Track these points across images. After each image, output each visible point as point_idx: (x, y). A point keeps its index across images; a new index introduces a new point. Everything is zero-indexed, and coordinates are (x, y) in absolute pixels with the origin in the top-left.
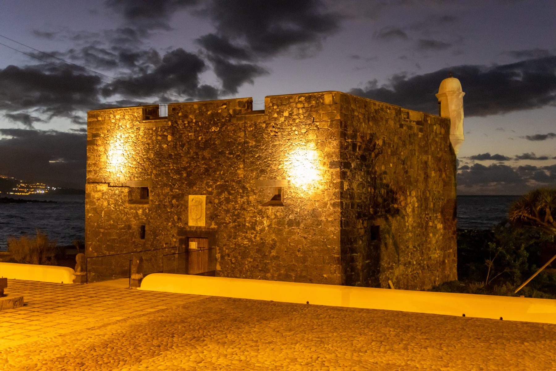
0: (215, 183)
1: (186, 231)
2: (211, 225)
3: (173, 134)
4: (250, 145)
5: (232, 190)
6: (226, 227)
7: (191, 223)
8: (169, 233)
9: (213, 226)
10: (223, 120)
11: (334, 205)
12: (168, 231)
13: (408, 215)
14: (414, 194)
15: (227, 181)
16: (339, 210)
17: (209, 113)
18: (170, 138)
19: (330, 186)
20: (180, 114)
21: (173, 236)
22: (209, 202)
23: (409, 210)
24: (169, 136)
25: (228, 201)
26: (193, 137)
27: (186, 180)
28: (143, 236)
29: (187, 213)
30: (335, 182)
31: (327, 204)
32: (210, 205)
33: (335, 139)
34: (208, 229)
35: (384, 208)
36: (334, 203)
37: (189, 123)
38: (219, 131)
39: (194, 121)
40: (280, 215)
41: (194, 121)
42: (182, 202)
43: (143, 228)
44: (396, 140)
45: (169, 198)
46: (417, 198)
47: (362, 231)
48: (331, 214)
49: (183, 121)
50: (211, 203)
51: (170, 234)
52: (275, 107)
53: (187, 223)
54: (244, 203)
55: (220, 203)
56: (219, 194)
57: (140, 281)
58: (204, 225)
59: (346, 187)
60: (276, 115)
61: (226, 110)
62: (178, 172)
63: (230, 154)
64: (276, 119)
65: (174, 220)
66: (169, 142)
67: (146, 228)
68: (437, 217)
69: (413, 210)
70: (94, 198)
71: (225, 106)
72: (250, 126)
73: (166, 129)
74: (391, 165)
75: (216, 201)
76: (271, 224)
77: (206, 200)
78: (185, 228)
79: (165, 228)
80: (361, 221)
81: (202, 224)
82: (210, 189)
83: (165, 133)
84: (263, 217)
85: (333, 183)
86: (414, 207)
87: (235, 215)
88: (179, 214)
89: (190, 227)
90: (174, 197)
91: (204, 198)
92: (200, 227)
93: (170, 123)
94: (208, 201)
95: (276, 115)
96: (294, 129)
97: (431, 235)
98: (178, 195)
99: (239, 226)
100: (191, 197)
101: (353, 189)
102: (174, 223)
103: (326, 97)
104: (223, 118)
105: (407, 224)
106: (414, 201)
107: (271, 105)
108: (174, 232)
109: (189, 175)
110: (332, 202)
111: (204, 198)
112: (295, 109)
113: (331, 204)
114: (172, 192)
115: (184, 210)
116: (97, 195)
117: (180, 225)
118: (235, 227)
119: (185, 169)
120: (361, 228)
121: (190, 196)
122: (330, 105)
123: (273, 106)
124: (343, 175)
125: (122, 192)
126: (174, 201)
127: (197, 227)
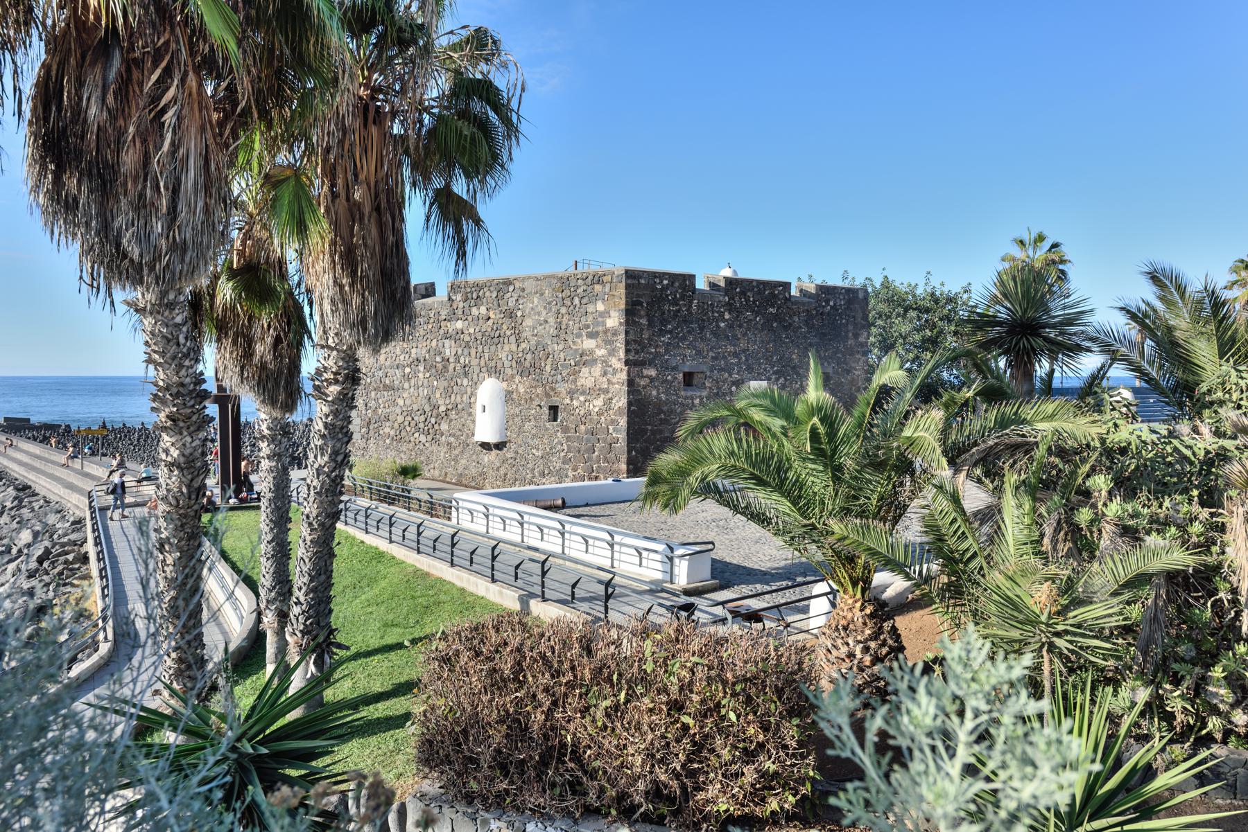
18: (727, 316)
119: (744, 351)
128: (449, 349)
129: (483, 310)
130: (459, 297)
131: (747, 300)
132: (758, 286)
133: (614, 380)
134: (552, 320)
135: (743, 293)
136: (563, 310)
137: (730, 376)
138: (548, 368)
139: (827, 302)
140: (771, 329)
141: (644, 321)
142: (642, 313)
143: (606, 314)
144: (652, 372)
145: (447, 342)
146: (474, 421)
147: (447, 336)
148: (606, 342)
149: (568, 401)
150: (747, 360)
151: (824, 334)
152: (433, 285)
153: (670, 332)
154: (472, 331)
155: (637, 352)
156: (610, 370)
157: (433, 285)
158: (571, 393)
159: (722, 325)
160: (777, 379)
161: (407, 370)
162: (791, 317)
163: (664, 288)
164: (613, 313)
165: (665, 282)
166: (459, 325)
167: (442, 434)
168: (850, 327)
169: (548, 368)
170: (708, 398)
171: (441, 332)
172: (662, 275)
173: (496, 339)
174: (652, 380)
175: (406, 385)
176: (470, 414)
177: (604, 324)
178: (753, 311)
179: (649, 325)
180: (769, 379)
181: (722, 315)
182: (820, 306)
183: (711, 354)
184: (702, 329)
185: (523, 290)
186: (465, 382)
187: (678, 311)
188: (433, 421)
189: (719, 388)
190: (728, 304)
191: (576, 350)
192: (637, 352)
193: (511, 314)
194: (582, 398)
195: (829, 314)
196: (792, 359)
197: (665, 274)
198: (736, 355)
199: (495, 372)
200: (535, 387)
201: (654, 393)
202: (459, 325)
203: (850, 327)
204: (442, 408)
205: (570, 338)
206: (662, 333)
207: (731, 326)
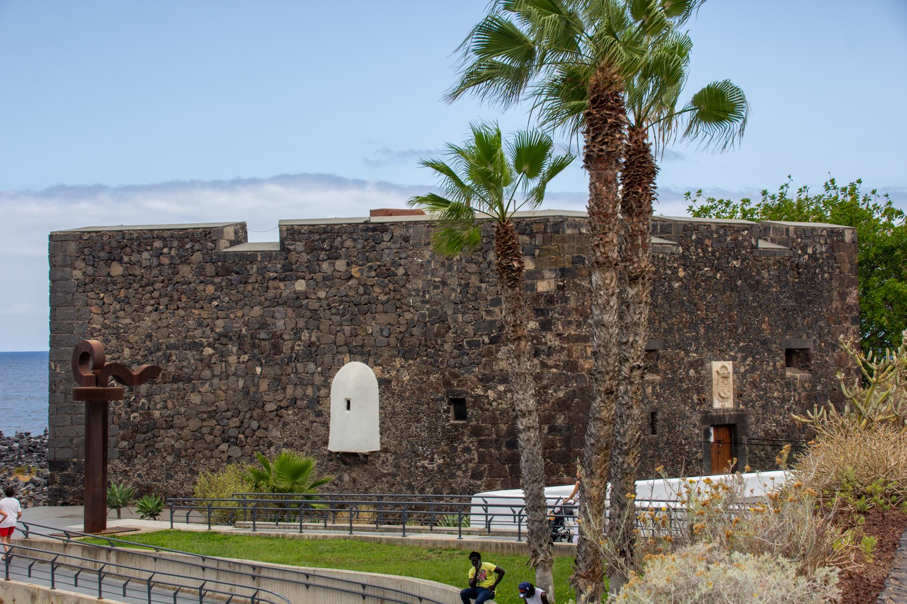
0: (737, 343)
1: (712, 416)
3: (685, 267)
4: (774, 290)
5: (758, 353)
6: (753, 407)
7: (717, 405)
8: (689, 421)
9: (741, 407)
10: (744, 252)
15: (751, 341)
18: (681, 274)
20: (694, 237)
21: (695, 425)
24: (680, 269)
34: (737, 411)
39: (710, 249)
42: (703, 372)
43: (653, 414)
51: (690, 424)
52: (799, 240)
53: (711, 405)
54: (770, 371)
62: (693, 326)
63: (753, 301)
66: (681, 280)
67: (659, 416)
70: (583, 370)
73: (675, 259)
76: (799, 400)
79: (684, 417)
81: (729, 404)
82: (732, 354)
83: (675, 265)
84: (790, 392)
87: (762, 389)
88: (699, 391)
89: (716, 410)
90: (692, 365)
91: (729, 365)
92: (728, 410)
93: (681, 249)
95: (800, 252)
98: (697, 361)
100: (716, 365)
102: (693, 407)
104: (744, 248)
108: (696, 418)
109: (708, 328)
111: (729, 365)
115: (707, 385)
117: (704, 407)
119: (703, 320)
121: (714, 363)
128: (282, 321)
129: (341, 265)
130: (300, 246)
131: (705, 251)
133: (550, 363)
134: (453, 282)
135: (700, 242)
136: (473, 268)
137: (687, 353)
138: (448, 347)
139: (804, 249)
140: (734, 288)
143: (536, 275)
145: (279, 311)
146: (326, 425)
147: (277, 302)
148: (538, 312)
149: (479, 391)
151: (802, 295)
152: (243, 226)
154: (322, 294)
155: (579, 325)
156: (543, 347)
157: (243, 226)
158: (486, 381)
159: (676, 285)
160: (744, 359)
161: (209, 351)
162: (759, 273)
164: (547, 274)
166: (300, 286)
167: (270, 445)
168: (835, 284)
169: (448, 347)
170: (661, 385)
171: (271, 293)
173: (361, 307)
175: (207, 373)
176: (319, 414)
177: (533, 287)
178: (712, 267)
180: (733, 359)
181: (675, 271)
182: (795, 254)
183: (664, 325)
185: (406, 239)
186: (311, 367)
188: (255, 425)
189: (674, 373)
190: (683, 257)
191: (492, 323)
193: (387, 274)
194: (501, 388)
195: (806, 266)
196: (762, 331)
199: (362, 353)
200: (428, 373)
202: (300, 286)
203: (835, 284)
204: (270, 407)
205: (482, 305)
207: (685, 287)
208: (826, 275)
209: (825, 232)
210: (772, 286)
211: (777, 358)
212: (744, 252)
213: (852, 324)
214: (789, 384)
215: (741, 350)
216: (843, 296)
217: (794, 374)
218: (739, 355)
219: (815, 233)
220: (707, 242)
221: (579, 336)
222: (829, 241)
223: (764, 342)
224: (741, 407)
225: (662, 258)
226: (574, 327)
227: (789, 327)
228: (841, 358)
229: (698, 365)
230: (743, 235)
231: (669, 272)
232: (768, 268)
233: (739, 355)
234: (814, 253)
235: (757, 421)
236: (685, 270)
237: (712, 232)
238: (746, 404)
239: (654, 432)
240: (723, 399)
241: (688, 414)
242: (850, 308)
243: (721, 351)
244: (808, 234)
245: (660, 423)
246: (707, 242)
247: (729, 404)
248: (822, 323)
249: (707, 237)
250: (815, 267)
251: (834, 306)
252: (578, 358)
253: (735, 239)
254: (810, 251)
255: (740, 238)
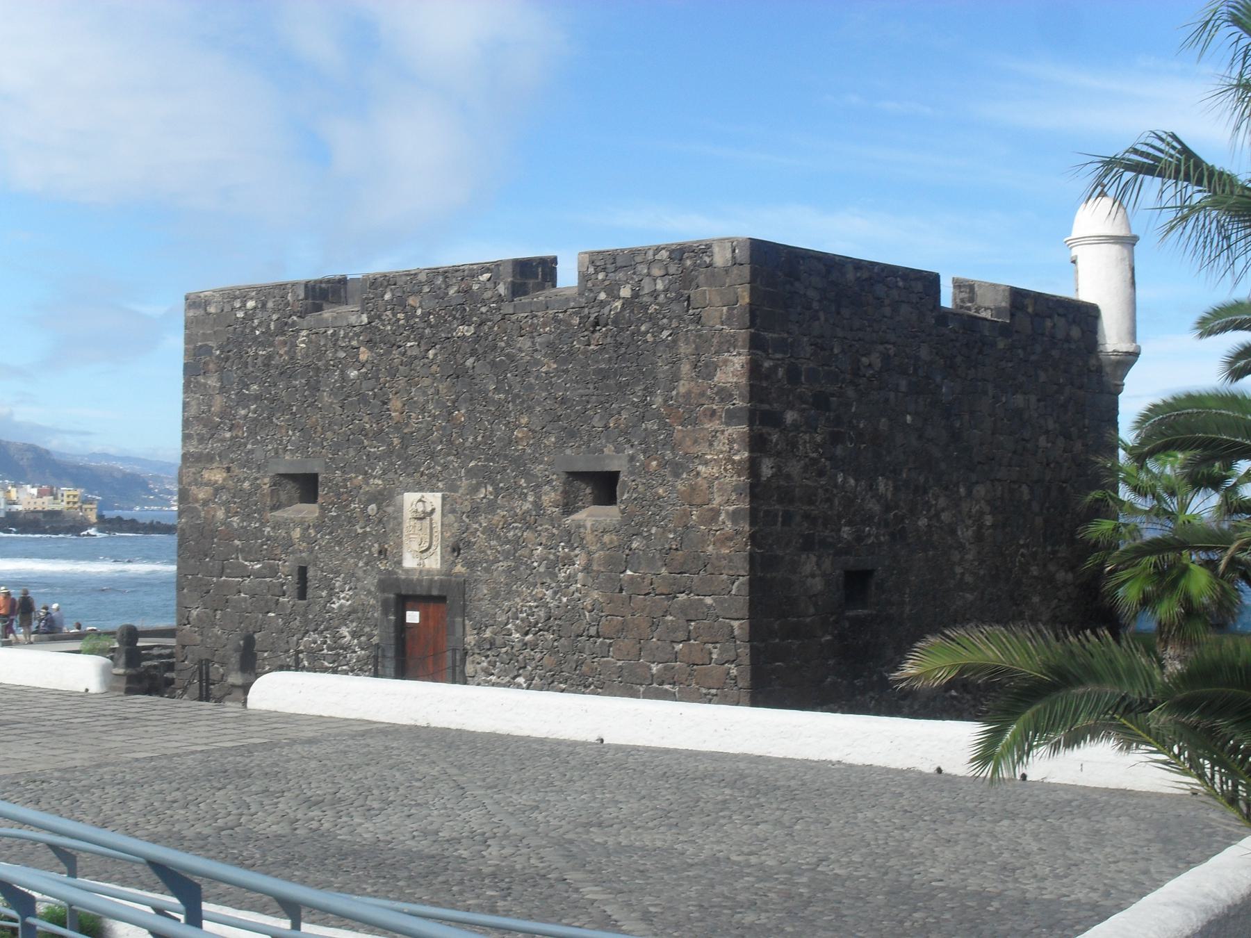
1: (397, 579)
2: (454, 563)
3: (371, 344)
4: (544, 369)
8: (359, 585)
9: (459, 568)
10: (484, 309)
11: (734, 516)
12: (358, 580)
13: (961, 547)
14: (983, 493)
15: (493, 460)
16: (747, 528)
17: (452, 292)
18: (364, 355)
19: (725, 470)
20: (387, 297)
21: (369, 592)
22: (449, 506)
23: (965, 533)
24: (362, 349)
25: (492, 507)
26: (415, 352)
27: (399, 457)
28: (302, 594)
29: (400, 537)
30: (737, 458)
31: (718, 513)
32: (451, 517)
33: (739, 354)
35: (887, 525)
36: (734, 512)
37: (407, 319)
38: (477, 338)
39: (419, 312)
40: (611, 542)
41: (419, 312)
42: (390, 509)
43: (302, 572)
44: (924, 353)
45: (360, 501)
46: (988, 502)
47: (817, 584)
48: (730, 539)
49: (394, 315)
50: (453, 511)
52: (601, 276)
53: (399, 563)
54: (528, 511)
55: (474, 512)
56: (475, 489)
57: (246, 688)
58: (439, 566)
59: (767, 470)
60: (602, 296)
61: (489, 285)
64: (603, 304)
65: (371, 554)
68: (1054, 552)
69: (979, 538)
70: (197, 501)
71: (487, 276)
72: (545, 325)
74: (909, 418)
75: (467, 506)
77: (443, 505)
78: (396, 573)
80: (814, 559)
81: (434, 563)
83: (354, 343)
85: (734, 462)
86: (980, 527)
87: (508, 542)
88: (382, 538)
89: (407, 571)
92: (429, 572)
94: (448, 507)
95: (602, 296)
96: (643, 328)
97: (1036, 599)
98: (380, 493)
99: (516, 568)
100: (410, 500)
101: (788, 477)
103: (716, 249)
105: (958, 570)
106: (982, 513)
107: (591, 270)
108: (371, 582)
110: (731, 508)
111: (434, 499)
112: (647, 280)
113: (727, 512)
114: (368, 484)
115: (394, 531)
116: (201, 496)
118: (509, 570)
119: (398, 427)
120: (813, 576)
122: (727, 270)
123: (596, 273)
124: (757, 444)
125: (259, 487)
126: (372, 508)
127: (421, 572)
132: (430, 282)
135: (400, 303)
139: (613, 293)
140: (459, 374)
141: (213, 382)
142: (212, 366)
144: (218, 476)
150: (404, 446)
153: (258, 398)
159: (353, 374)
163: (249, 317)
165: (251, 304)
168: (684, 349)
170: (319, 527)
172: (242, 294)
174: (218, 490)
179: (223, 390)
184: (315, 388)
187: (270, 357)
192: (201, 440)
197: (252, 288)
198: (379, 435)
201: (220, 514)
206: (243, 400)
208: (665, 333)
209: (664, 254)
210: (537, 363)
211: (547, 488)
212: (484, 309)
213: (728, 424)
214: (572, 537)
215: (471, 473)
216: (705, 370)
217: (591, 516)
218: (465, 483)
219: (638, 259)
220: (412, 301)
221: (201, 454)
222: (672, 269)
223: (519, 463)
224: (459, 568)
225: (333, 334)
226: (195, 443)
227: (572, 435)
228: (693, 488)
229: (384, 498)
230: (479, 282)
231: (342, 354)
232: (533, 332)
233: (465, 483)
234: (636, 295)
235: (496, 595)
236: (371, 349)
237: (421, 284)
238: (471, 565)
239: (302, 594)
240: (420, 556)
241: (360, 573)
242: (724, 394)
243: (431, 476)
244: (620, 263)
245: (312, 583)
246: (412, 301)
247: (434, 563)
248: (652, 425)
249: (413, 293)
250: (640, 322)
251: (682, 390)
252: (190, 484)
253: (467, 291)
254: (626, 292)
255: (475, 287)
